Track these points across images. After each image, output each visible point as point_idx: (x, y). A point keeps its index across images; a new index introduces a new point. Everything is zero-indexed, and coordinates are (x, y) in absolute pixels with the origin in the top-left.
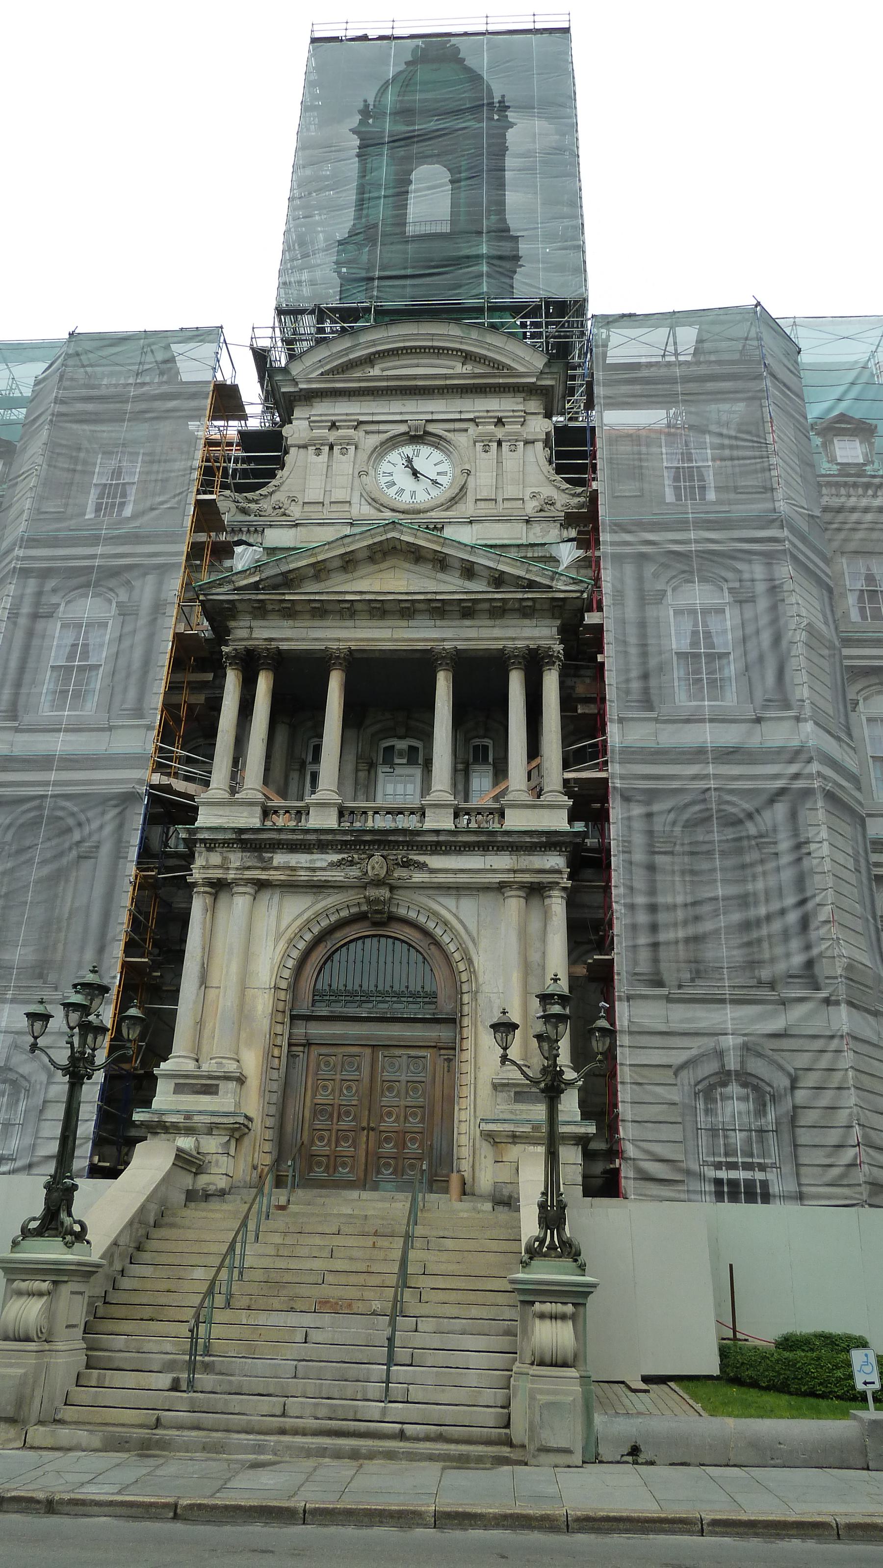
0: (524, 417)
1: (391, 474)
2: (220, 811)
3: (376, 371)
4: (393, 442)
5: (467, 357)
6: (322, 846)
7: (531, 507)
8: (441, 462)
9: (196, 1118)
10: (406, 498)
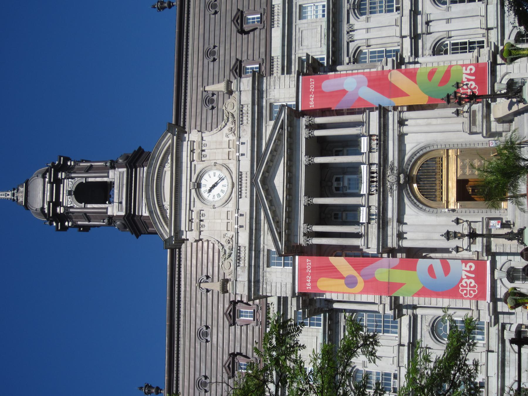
1: (214, 196)
2: (370, 239)
3: (166, 204)
5: (162, 166)
6: (385, 200)
7: (232, 137)
10: (225, 189)
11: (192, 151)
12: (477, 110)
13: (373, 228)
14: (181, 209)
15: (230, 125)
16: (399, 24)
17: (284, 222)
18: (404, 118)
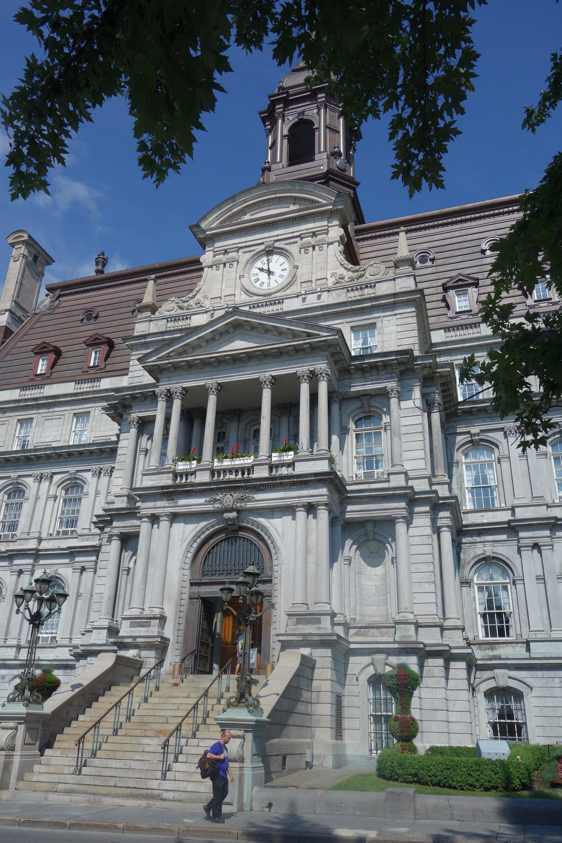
0: (327, 229)
2: (153, 477)
3: (247, 217)
4: (258, 256)
5: (296, 200)
8: (284, 263)
9: (138, 640)
10: (265, 287)
11: (314, 234)
12: (321, 626)
13: (166, 480)
14: (240, 237)
15: (347, 275)
16: (535, 502)
17: (180, 359)
18: (318, 511)
